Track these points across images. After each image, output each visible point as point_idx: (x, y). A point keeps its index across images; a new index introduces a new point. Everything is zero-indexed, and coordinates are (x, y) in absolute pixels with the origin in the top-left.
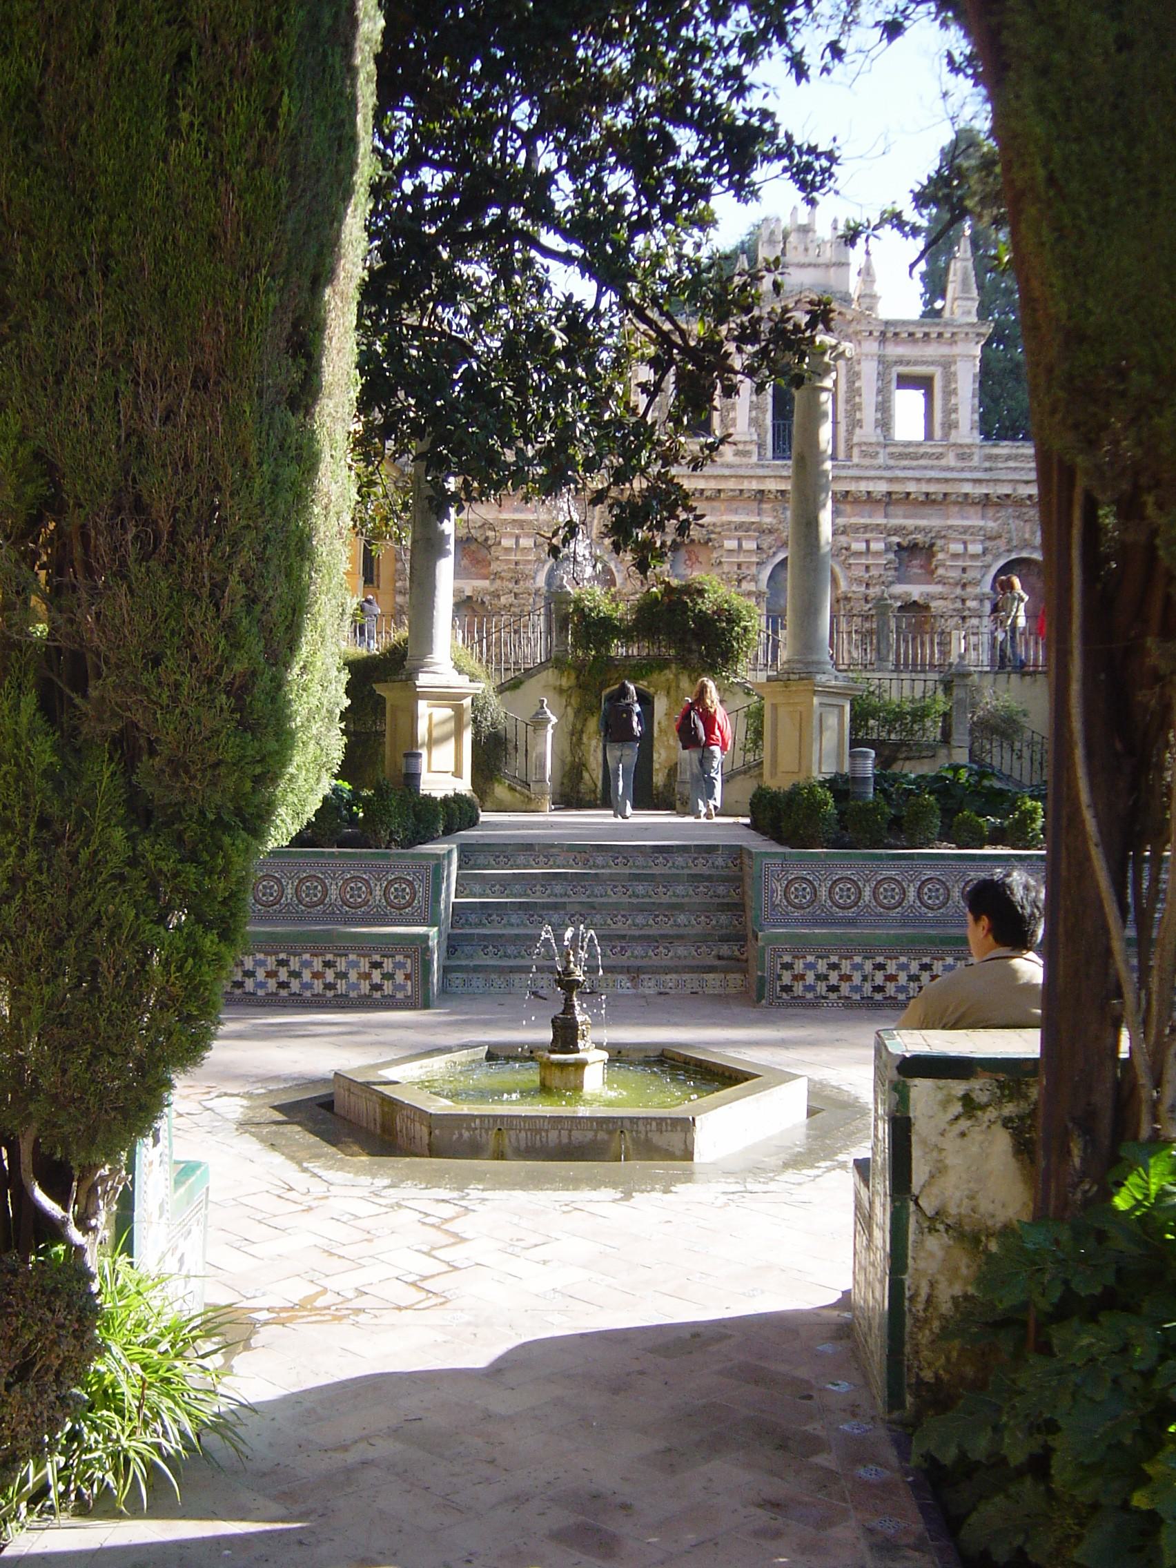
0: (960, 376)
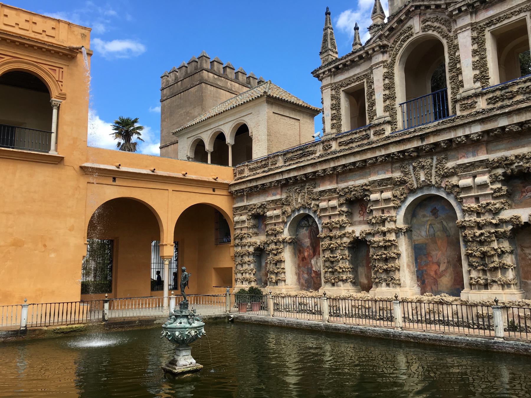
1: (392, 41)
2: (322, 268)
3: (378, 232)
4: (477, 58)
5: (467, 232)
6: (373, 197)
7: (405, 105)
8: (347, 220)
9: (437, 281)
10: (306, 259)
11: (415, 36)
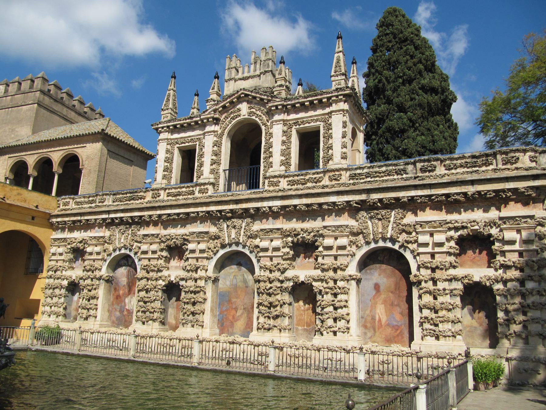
0: (333, 126)
1: (224, 116)
2: (135, 306)
3: (191, 279)
4: (284, 147)
5: (262, 284)
6: (191, 246)
7: (227, 172)
8: (165, 264)
9: (233, 325)
10: (120, 297)
11: (242, 117)
